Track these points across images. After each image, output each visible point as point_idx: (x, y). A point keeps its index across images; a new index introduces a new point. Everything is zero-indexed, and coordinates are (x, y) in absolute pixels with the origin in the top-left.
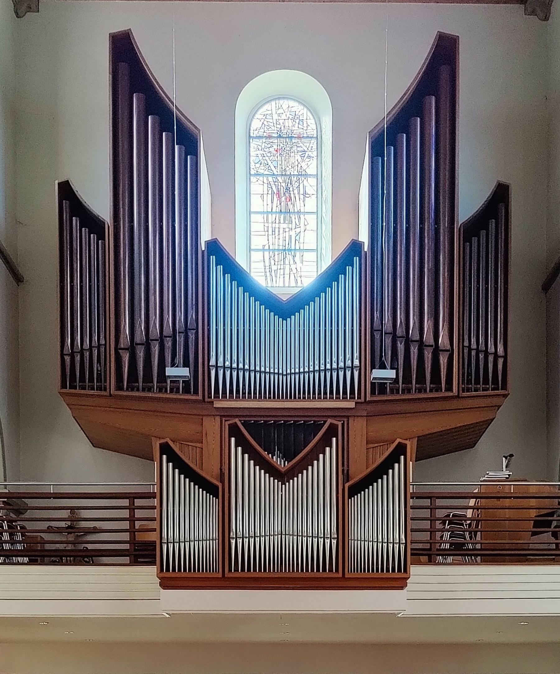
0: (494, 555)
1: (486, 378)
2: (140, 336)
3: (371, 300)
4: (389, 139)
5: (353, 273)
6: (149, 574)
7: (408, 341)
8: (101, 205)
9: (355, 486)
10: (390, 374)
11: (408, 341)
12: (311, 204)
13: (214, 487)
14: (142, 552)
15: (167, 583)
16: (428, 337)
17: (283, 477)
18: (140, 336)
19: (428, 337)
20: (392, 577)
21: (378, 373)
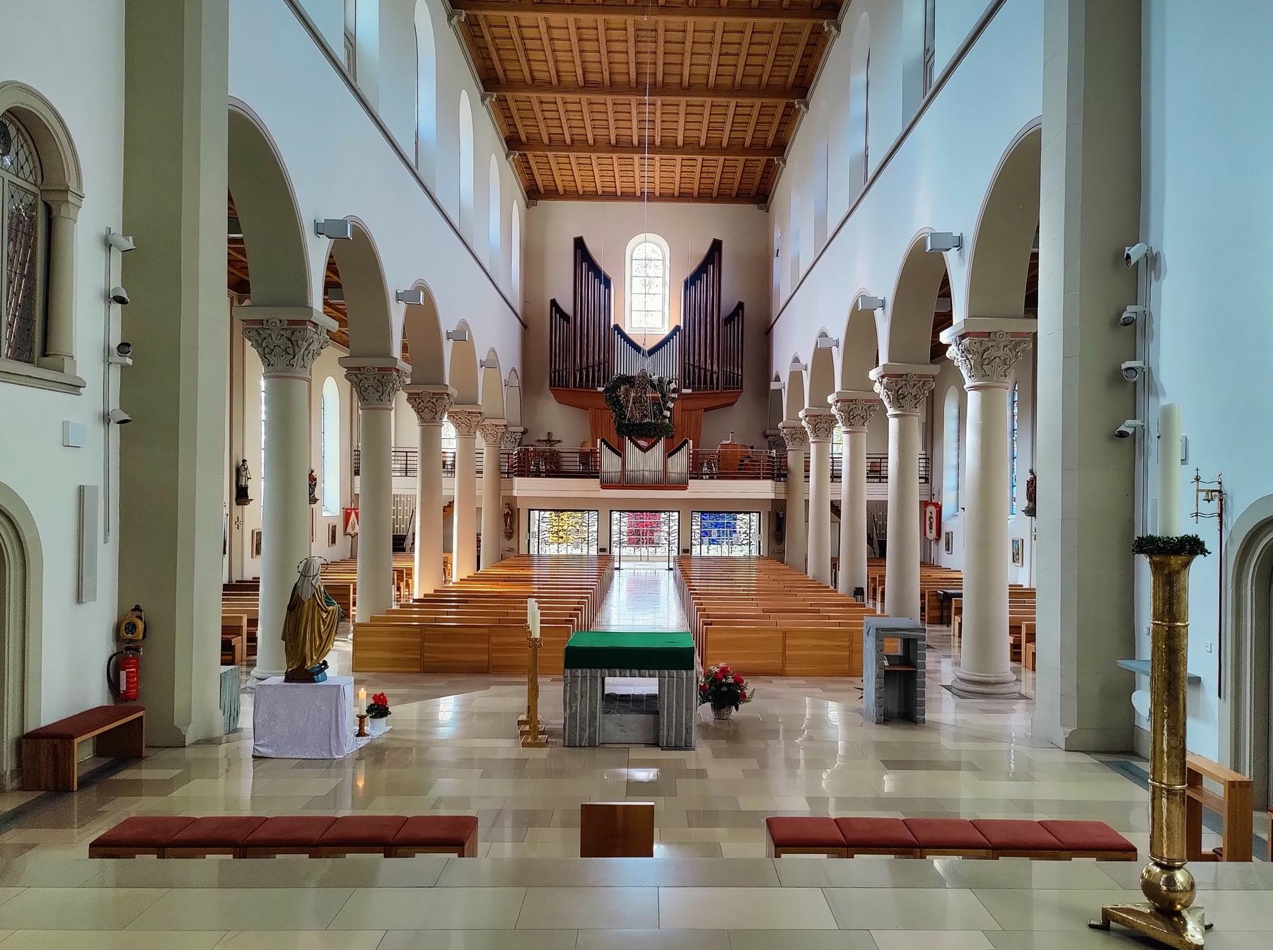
0: (721, 477)
1: (733, 385)
2: (584, 365)
3: (684, 352)
4: (691, 282)
5: (677, 338)
6: (595, 483)
7: (700, 369)
8: (567, 307)
9: (670, 453)
10: (690, 391)
11: (700, 369)
12: (660, 290)
13: (620, 452)
14: (588, 468)
15: (603, 487)
16: (709, 367)
17: (644, 450)
18: (584, 365)
19: (709, 367)
20: (682, 486)
21: (684, 391)
